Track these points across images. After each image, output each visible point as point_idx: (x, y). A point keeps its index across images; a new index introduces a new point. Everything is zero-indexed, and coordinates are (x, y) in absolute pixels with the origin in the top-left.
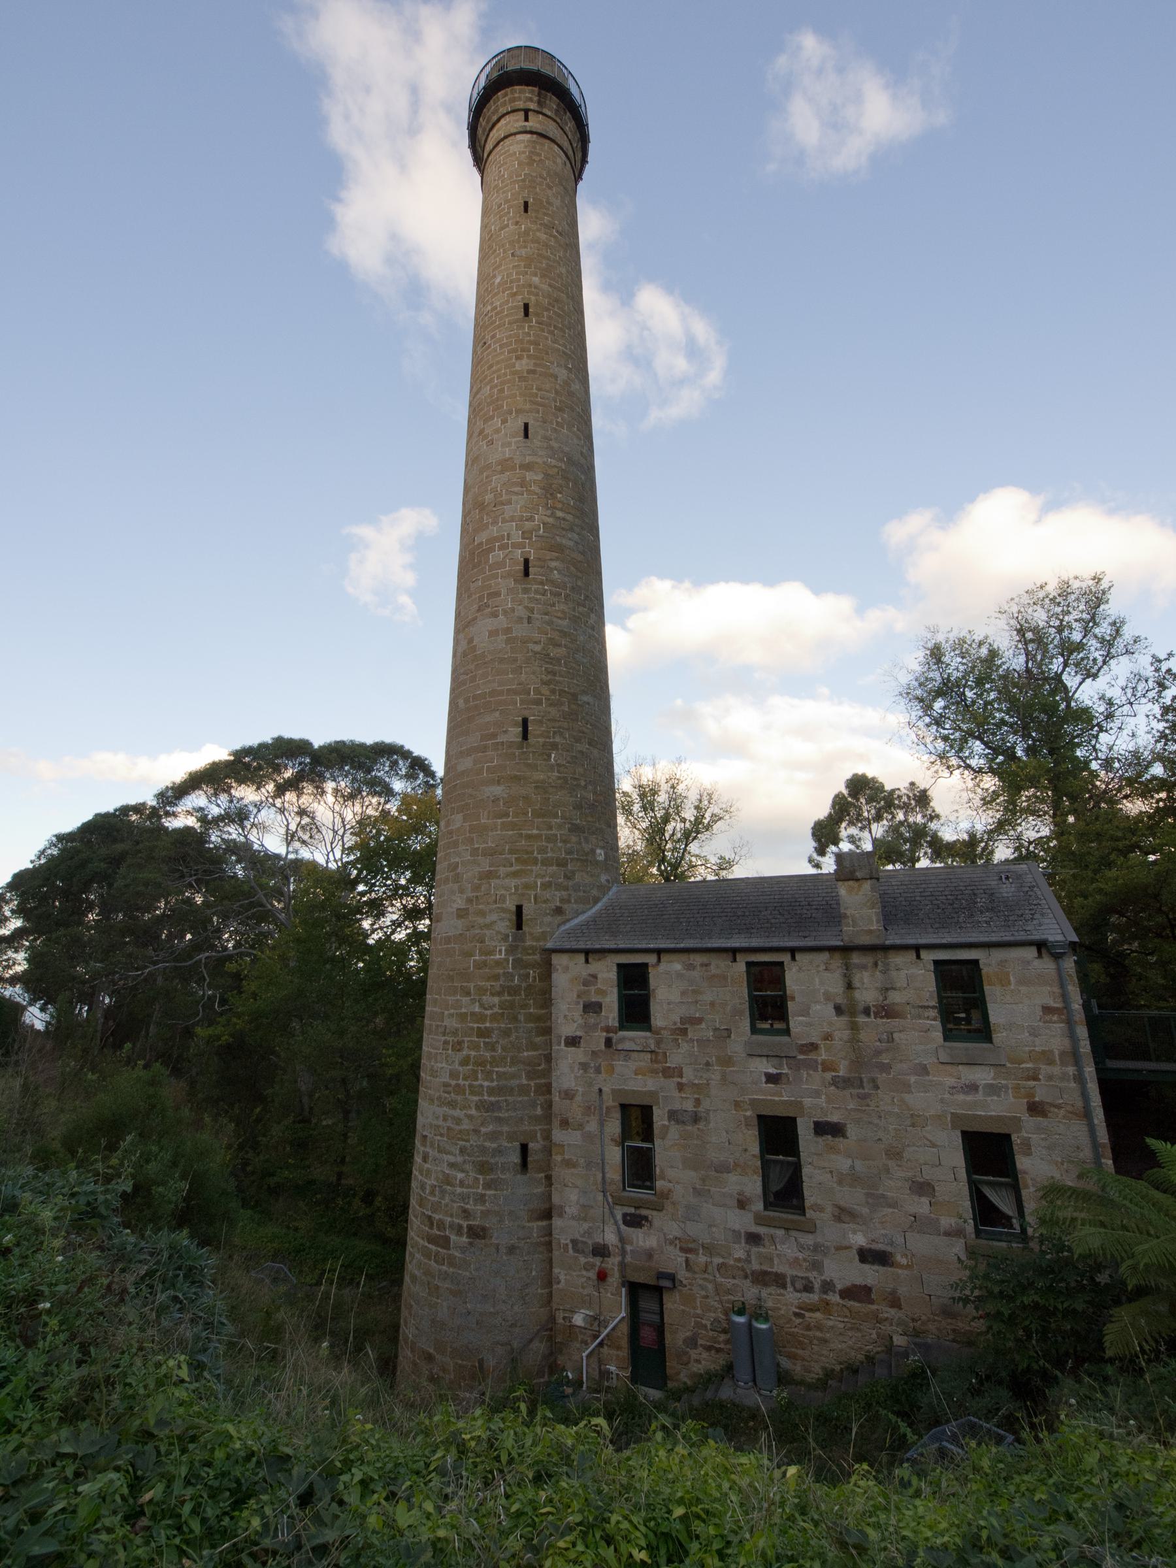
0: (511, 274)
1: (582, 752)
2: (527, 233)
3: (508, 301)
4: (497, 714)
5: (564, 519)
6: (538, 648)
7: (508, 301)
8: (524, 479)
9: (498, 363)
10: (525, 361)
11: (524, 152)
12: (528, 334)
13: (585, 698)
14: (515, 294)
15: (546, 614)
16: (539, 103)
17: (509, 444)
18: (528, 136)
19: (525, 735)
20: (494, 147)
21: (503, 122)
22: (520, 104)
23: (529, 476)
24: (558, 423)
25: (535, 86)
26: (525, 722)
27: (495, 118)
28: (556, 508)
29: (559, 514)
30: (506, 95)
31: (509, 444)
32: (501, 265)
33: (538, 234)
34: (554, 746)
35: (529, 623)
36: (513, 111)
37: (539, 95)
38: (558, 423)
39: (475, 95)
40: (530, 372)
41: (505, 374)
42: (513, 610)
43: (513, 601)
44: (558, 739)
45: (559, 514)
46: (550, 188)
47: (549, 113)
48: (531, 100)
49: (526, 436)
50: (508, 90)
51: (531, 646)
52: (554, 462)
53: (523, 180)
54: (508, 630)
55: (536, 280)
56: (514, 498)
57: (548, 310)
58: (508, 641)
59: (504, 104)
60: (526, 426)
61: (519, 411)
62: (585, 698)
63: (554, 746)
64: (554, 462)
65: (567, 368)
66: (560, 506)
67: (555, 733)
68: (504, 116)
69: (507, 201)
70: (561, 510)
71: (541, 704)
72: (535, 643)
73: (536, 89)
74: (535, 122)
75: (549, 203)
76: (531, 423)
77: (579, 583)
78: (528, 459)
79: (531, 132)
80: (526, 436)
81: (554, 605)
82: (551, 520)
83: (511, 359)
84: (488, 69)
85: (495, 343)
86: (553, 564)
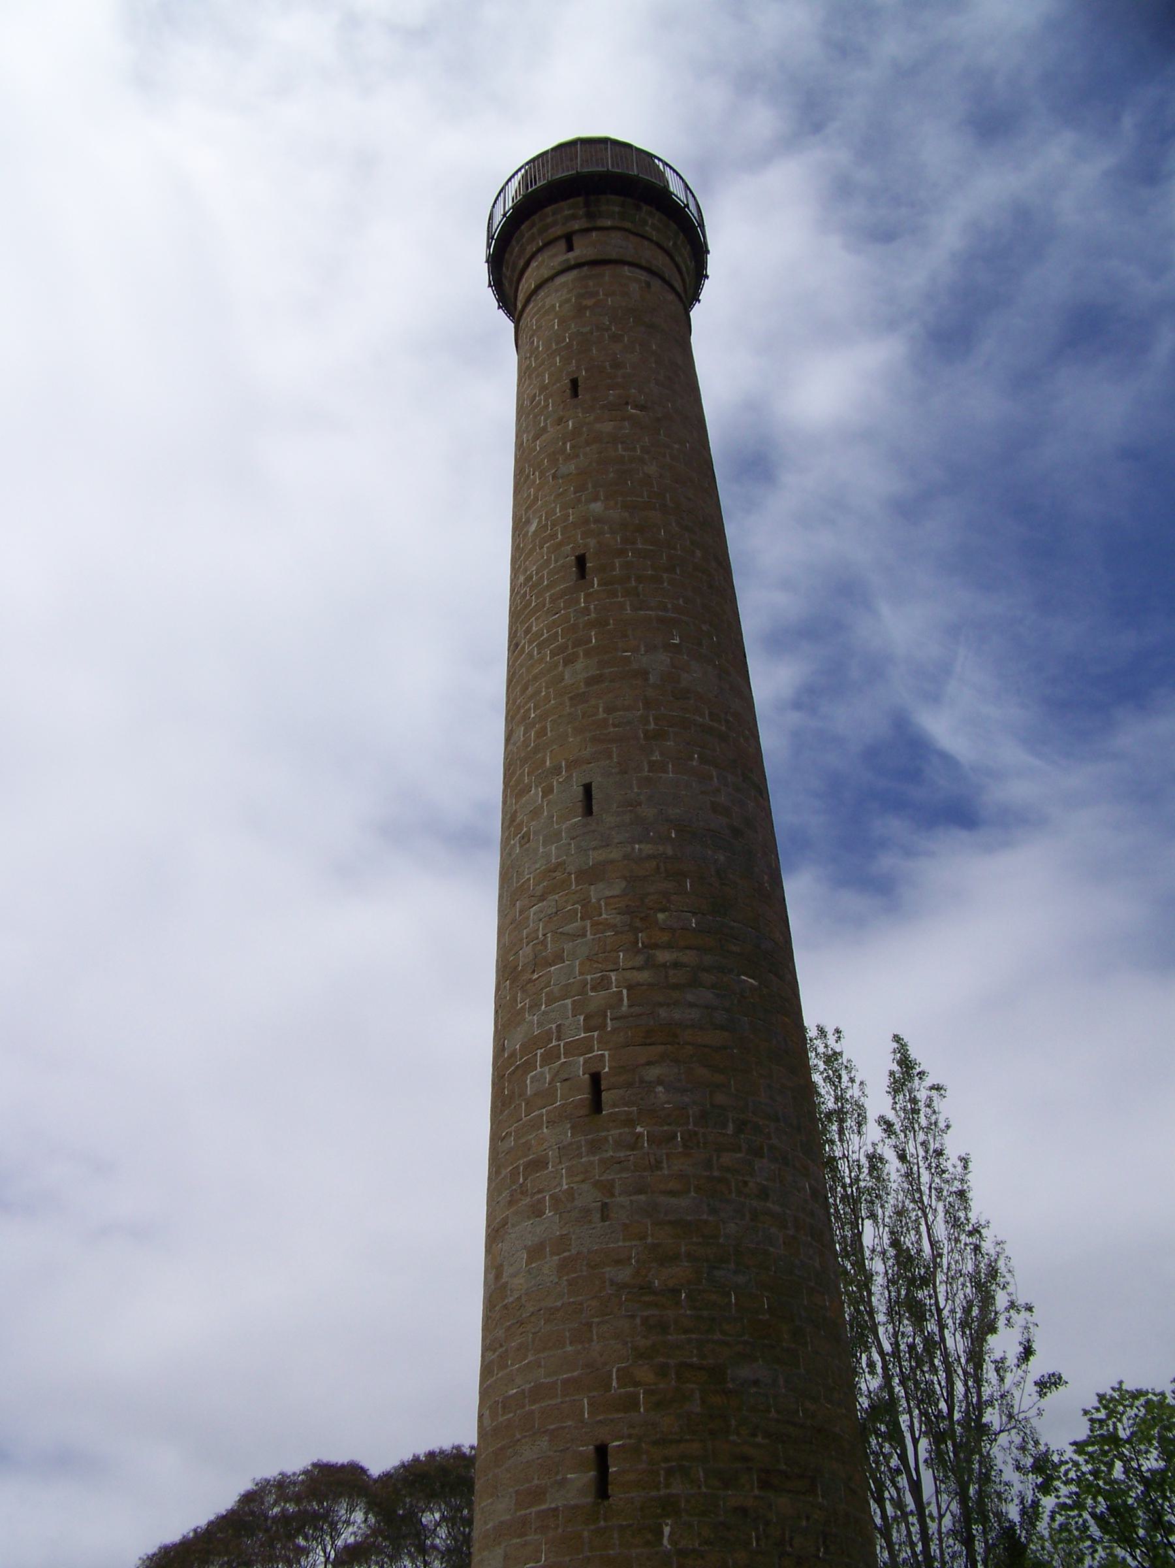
0: (554, 511)
1: (743, 1511)
2: (576, 432)
3: (548, 561)
4: (544, 1443)
5: (676, 965)
6: (624, 1274)
7: (548, 561)
8: (585, 902)
9: (535, 678)
10: (579, 665)
11: (568, 301)
12: (586, 611)
13: (745, 1372)
14: (561, 544)
15: (640, 1192)
16: (590, 216)
17: (557, 836)
18: (573, 274)
19: (602, 1489)
20: (539, 287)
21: (534, 264)
22: (558, 231)
23: (595, 893)
24: (652, 765)
25: (579, 195)
26: (602, 1451)
27: (522, 263)
28: (656, 946)
29: (663, 956)
30: (533, 225)
31: (557, 836)
32: (536, 499)
33: (598, 426)
34: (669, 1507)
35: (604, 1218)
36: (547, 244)
37: (587, 204)
38: (652, 765)
39: (498, 217)
40: (590, 682)
41: (547, 699)
42: (570, 1193)
43: (571, 1173)
44: (677, 1488)
45: (663, 956)
46: (616, 338)
47: (609, 223)
48: (574, 217)
49: (588, 811)
50: (535, 218)
51: (609, 1271)
52: (648, 849)
53: (569, 346)
54: (562, 1243)
55: (597, 507)
56: (568, 947)
57: (621, 553)
58: (563, 1267)
59: (533, 239)
60: (588, 789)
61: (573, 764)
62: (745, 1372)
63: (669, 1507)
64: (648, 849)
65: (668, 647)
66: (665, 938)
67: (670, 1472)
68: (533, 256)
69: (543, 388)
70: (668, 946)
71: (636, 1405)
72: (618, 1262)
73: (580, 199)
74: (583, 250)
75: (617, 365)
76: (597, 782)
77: (720, 1098)
78: (594, 857)
79: (578, 266)
80: (588, 811)
81: (658, 1165)
82: (644, 976)
83: (556, 666)
84: (515, 183)
85: (530, 642)
86: (653, 1073)
